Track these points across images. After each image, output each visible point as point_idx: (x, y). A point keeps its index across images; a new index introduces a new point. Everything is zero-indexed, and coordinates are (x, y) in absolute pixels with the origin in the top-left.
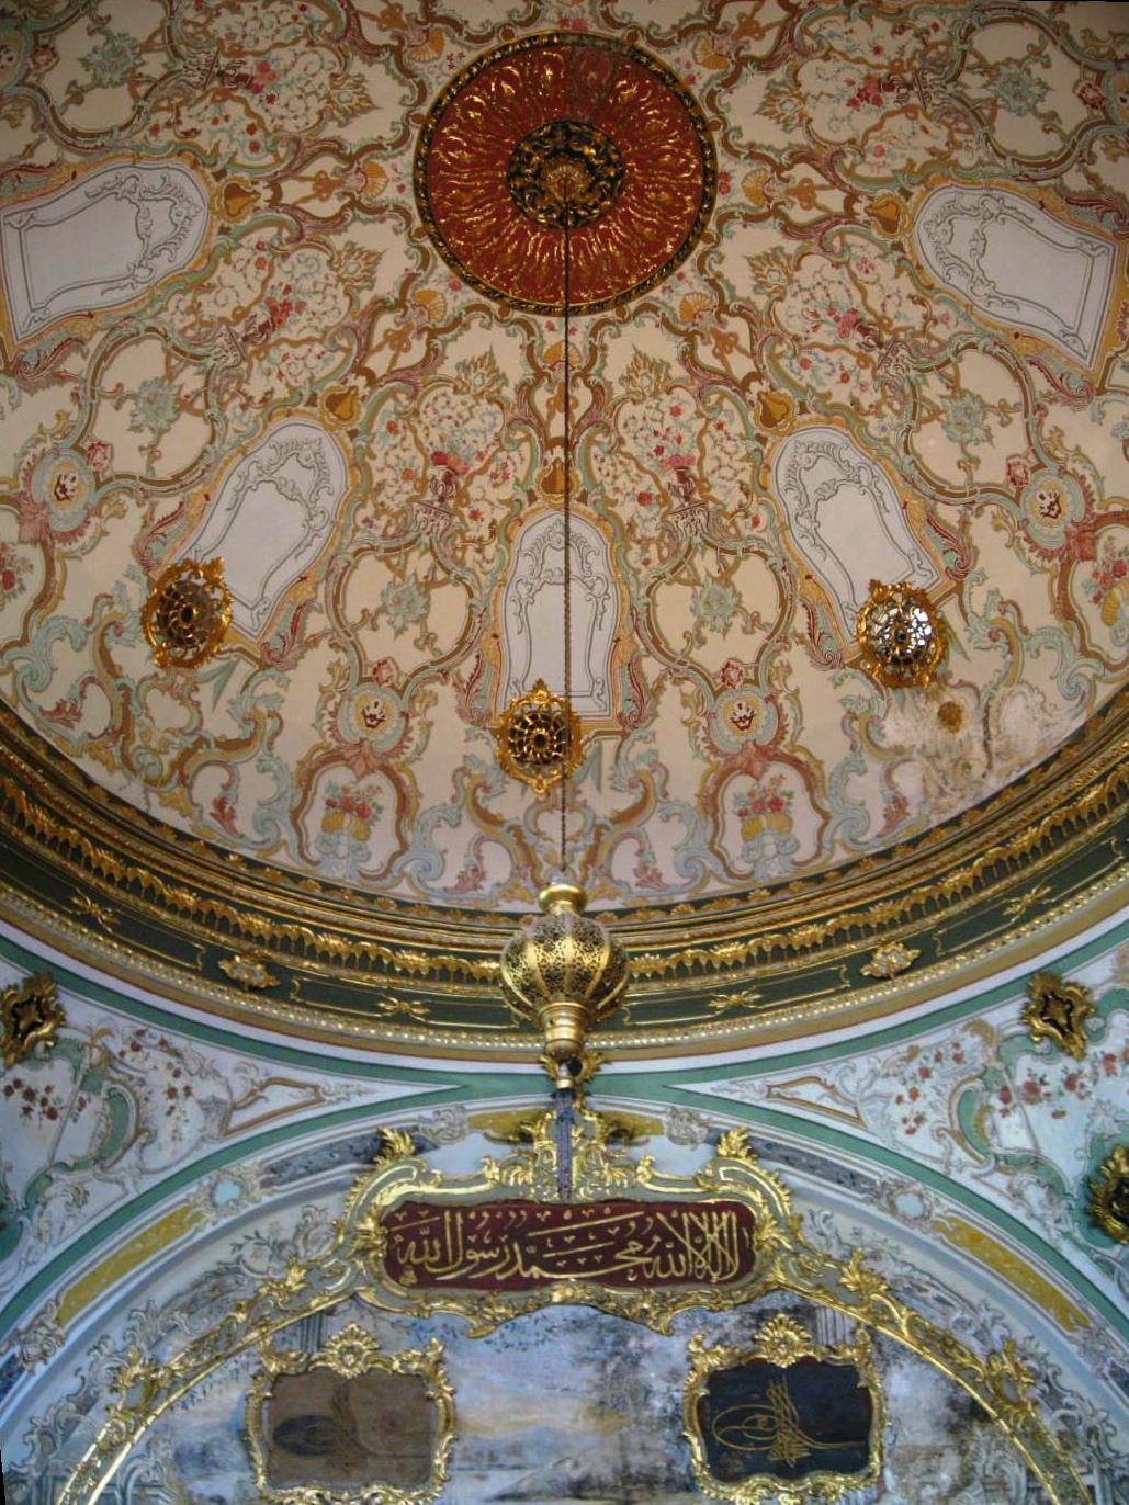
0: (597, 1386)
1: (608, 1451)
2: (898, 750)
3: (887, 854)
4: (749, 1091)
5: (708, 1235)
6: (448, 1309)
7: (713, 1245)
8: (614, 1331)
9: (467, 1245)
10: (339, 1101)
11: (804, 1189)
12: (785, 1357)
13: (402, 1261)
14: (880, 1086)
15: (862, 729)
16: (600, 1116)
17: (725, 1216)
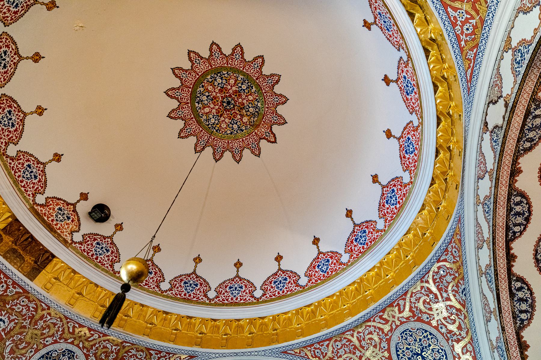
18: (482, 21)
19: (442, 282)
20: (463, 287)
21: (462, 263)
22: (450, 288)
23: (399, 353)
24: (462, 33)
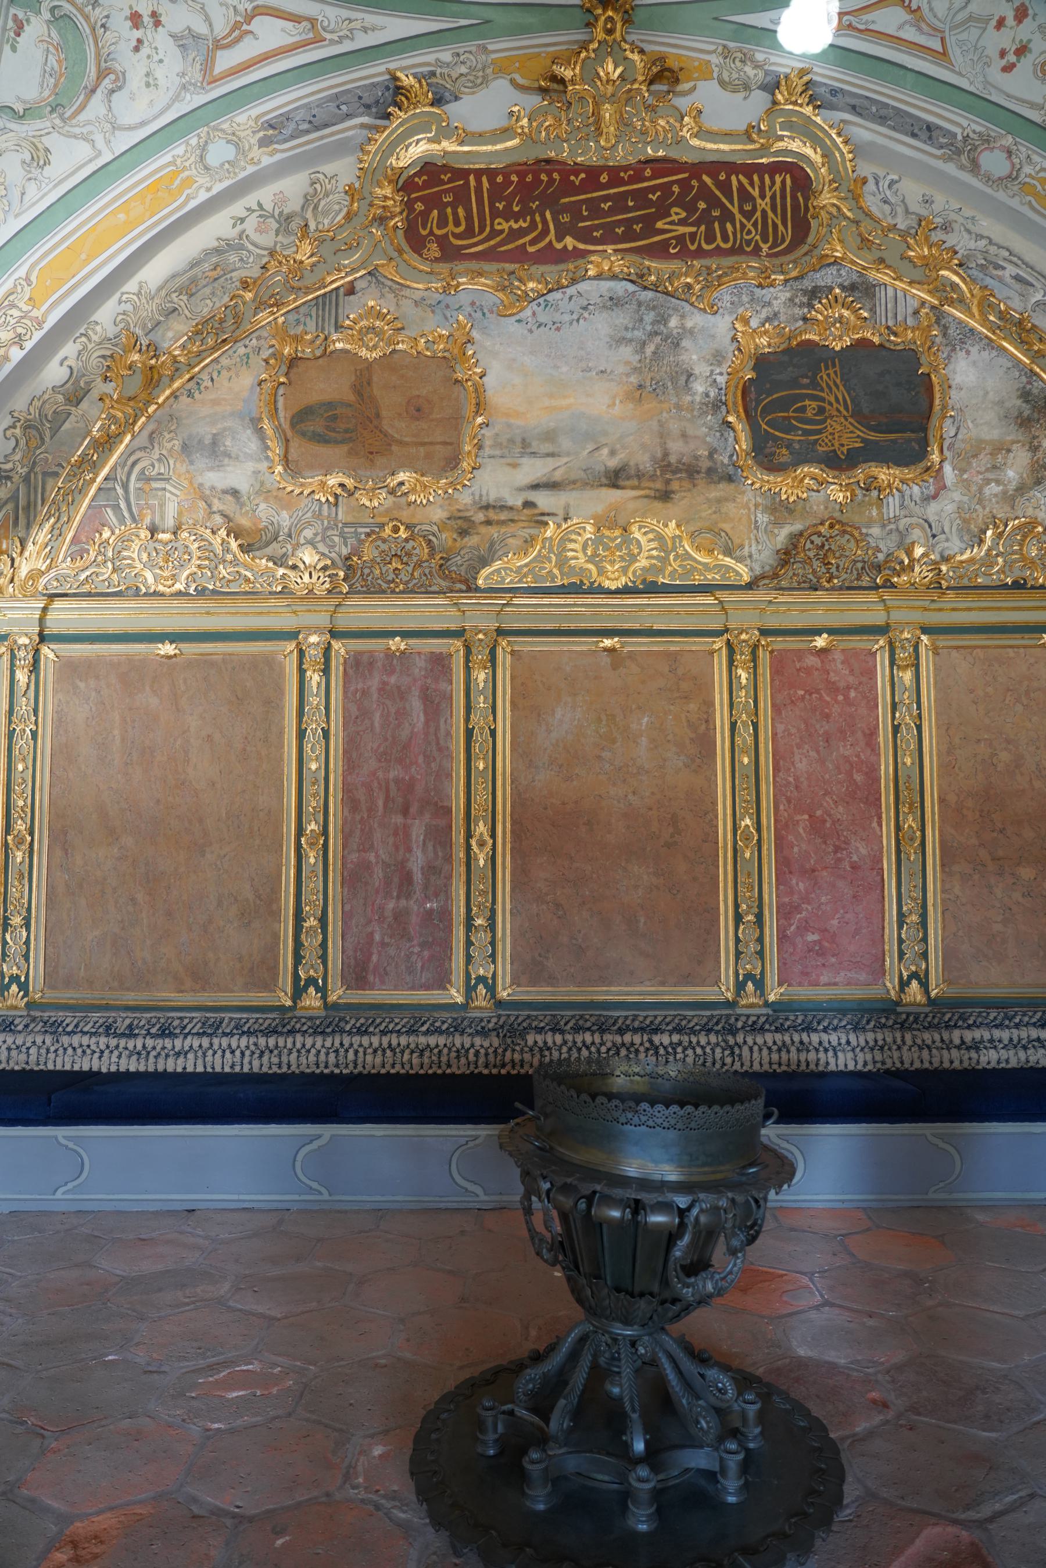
0: (635, 369)
1: (647, 438)
5: (759, 201)
6: (476, 286)
7: (764, 211)
8: (654, 308)
9: (495, 214)
10: (341, 40)
11: (872, 144)
12: (841, 339)
13: (424, 233)
16: (642, 52)
17: (778, 179)
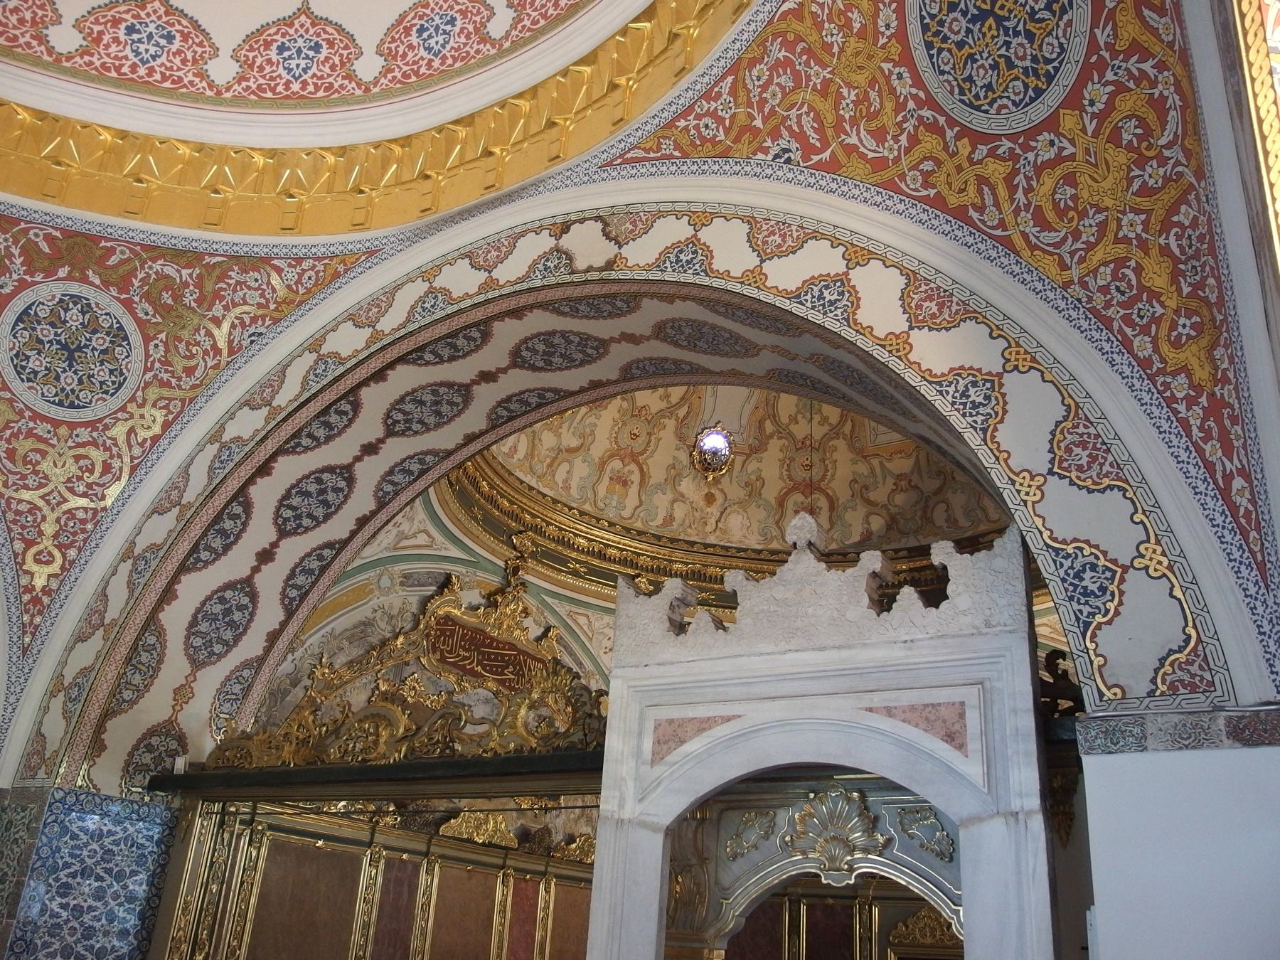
2: (682, 495)
3: (659, 538)
4: (563, 608)
14: (607, 630)
15: (673, 478)
18: (725, 154)
19: (235, 291)
20: (263, 330)
21: (300, 303)
22: (238, 310)
23: (25, 318)
24: (699, 117)
